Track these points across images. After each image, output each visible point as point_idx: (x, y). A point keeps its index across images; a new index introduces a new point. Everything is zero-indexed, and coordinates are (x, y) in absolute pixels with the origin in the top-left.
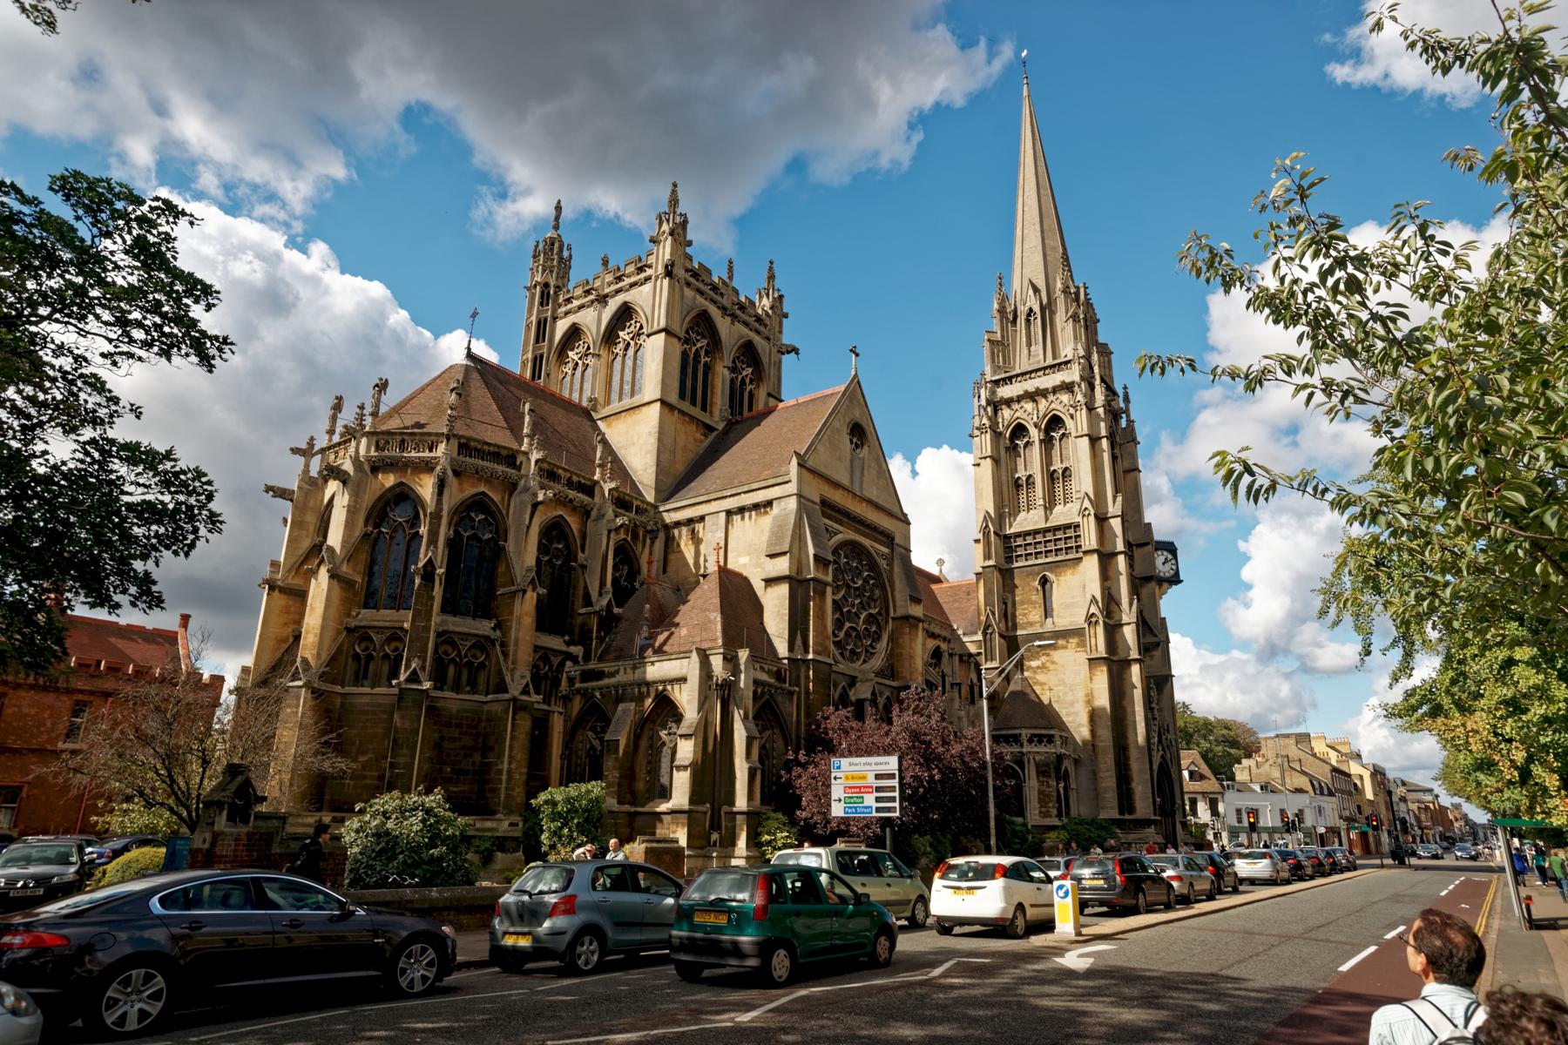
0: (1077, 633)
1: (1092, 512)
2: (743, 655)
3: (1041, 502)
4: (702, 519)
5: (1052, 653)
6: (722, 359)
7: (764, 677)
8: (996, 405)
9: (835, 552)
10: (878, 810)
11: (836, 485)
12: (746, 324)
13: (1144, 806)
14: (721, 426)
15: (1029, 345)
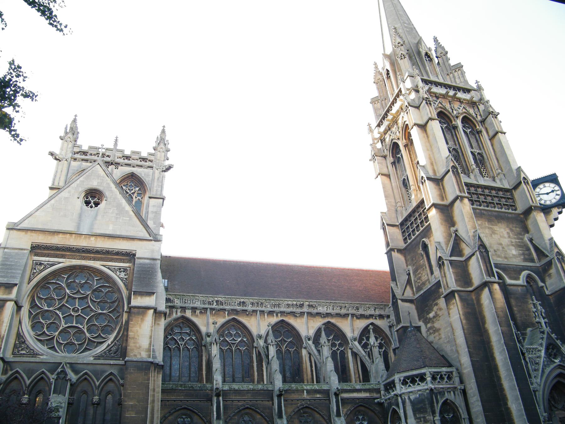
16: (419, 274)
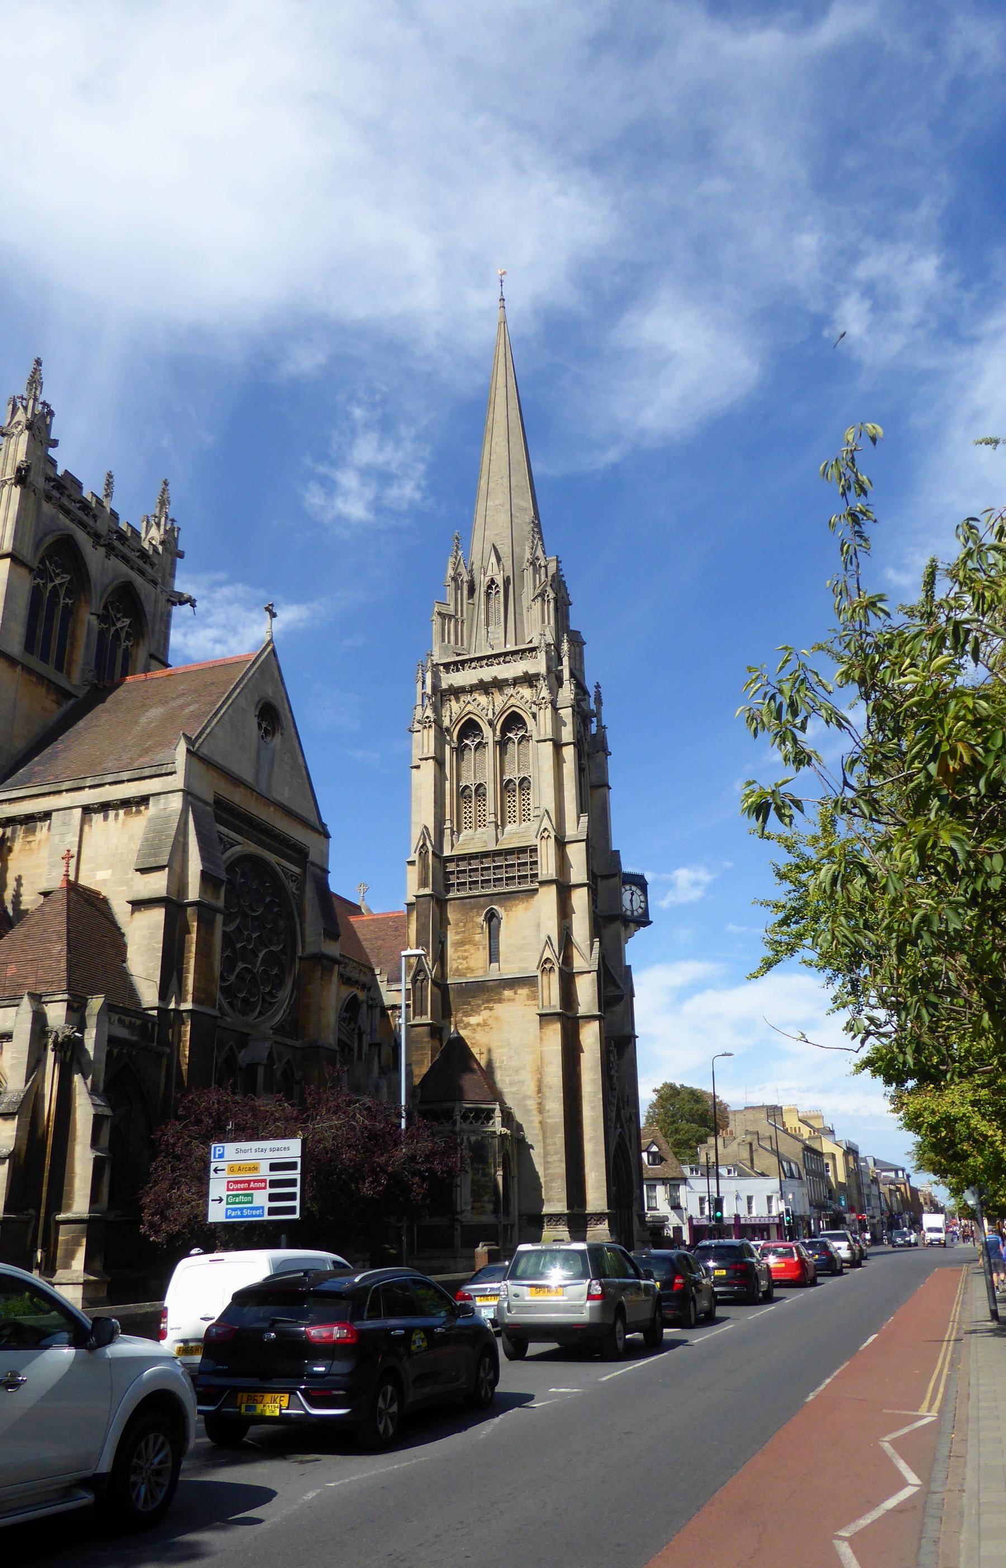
0: (529, 981)
1: (553, 834)
2: (96, 1003)
3: (492, 818)
4: (47, 815)
5: (496, 1006)
6: (88, 602)
7: (123, 1033)
8: (441, 696)
9: (230, 868)
10: (272, 1211)
11: (236, 781)
12: (125, 559)
13: (596, 1198)
14: (81, 693)
15: (488, 625)
16: (465, 951)
